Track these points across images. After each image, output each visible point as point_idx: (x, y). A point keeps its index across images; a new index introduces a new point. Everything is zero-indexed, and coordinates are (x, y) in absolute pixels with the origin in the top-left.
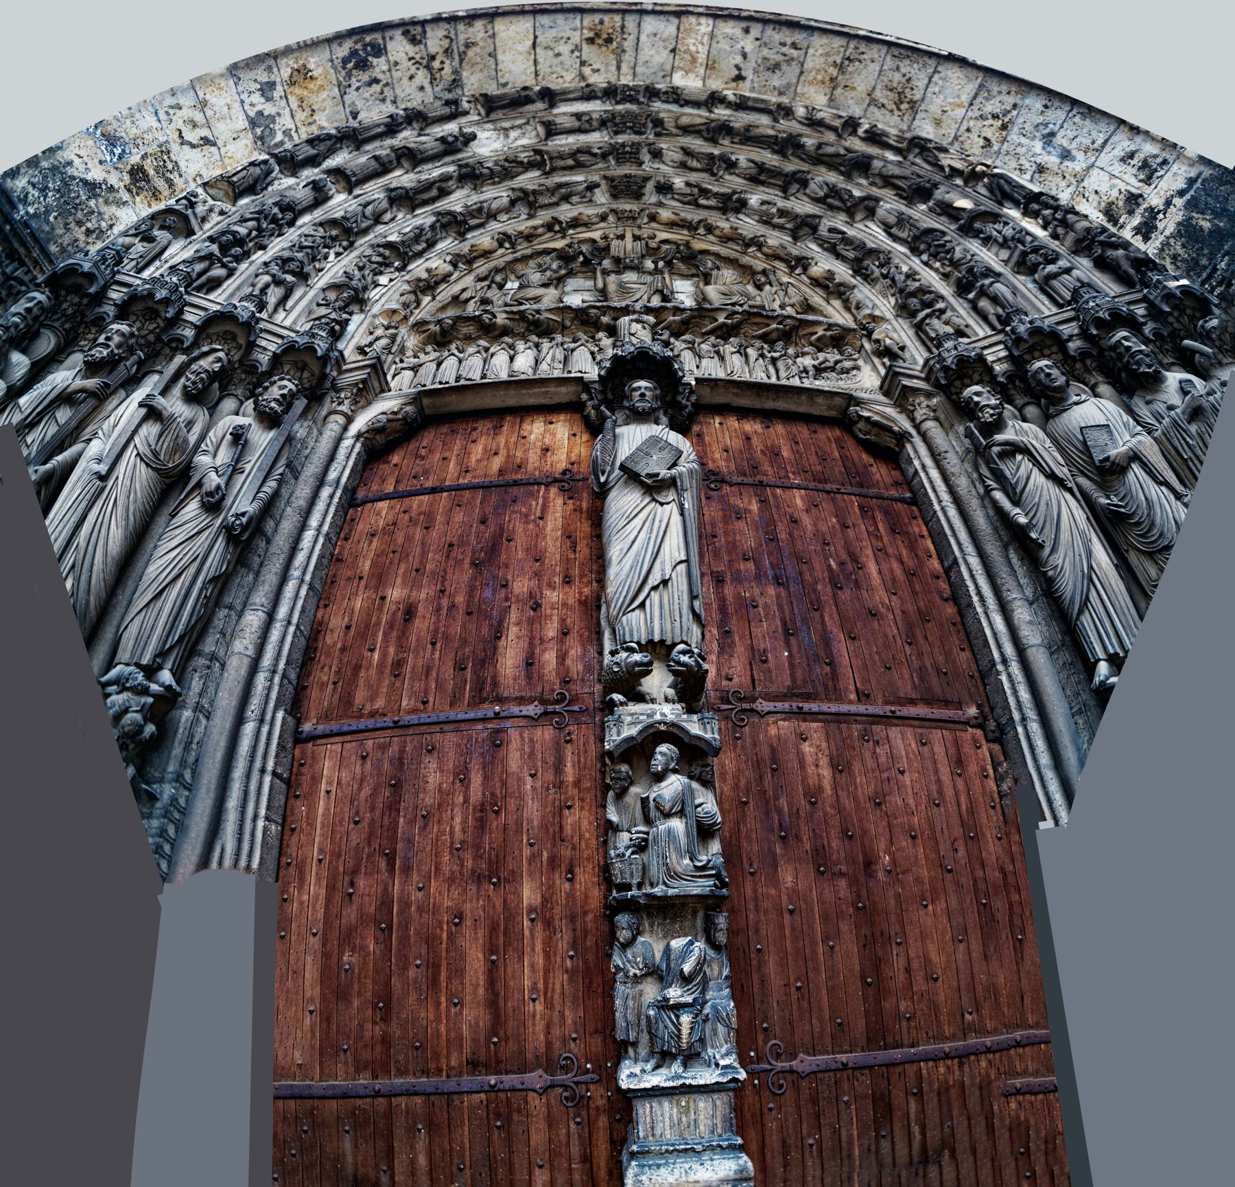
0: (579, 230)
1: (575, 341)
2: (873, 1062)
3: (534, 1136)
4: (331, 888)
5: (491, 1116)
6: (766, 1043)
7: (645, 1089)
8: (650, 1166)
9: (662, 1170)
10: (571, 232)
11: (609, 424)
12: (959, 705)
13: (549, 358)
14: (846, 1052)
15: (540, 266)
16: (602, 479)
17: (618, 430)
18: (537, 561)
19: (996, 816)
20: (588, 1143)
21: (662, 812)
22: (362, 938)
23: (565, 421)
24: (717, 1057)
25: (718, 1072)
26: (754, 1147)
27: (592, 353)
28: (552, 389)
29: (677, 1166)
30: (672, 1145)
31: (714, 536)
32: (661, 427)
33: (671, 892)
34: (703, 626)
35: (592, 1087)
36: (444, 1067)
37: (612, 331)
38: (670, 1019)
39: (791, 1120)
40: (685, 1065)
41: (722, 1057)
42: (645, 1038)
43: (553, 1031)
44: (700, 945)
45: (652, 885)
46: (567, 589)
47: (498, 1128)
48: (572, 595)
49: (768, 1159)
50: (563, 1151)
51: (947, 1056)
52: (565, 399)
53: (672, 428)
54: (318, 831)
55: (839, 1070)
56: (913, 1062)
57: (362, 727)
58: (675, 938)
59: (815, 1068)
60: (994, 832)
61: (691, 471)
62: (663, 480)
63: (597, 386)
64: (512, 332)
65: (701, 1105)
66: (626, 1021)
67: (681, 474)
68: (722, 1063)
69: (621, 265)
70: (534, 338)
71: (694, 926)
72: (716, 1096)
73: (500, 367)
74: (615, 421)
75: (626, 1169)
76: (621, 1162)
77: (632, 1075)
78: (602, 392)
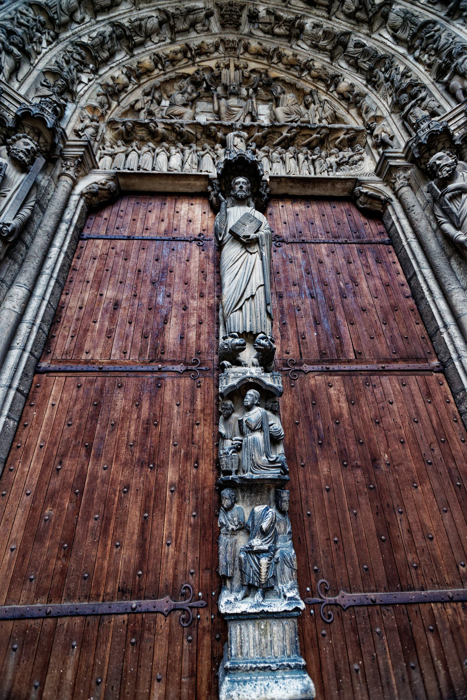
0: (203, 58)
1: (203, 150)
2: (394, 601)
3: (157, 652)
4: (46, 465)
5: (129, 634)
6: (317, 581)
7: (237, 614)
8: (238, 682)
9: (248, 686)
10: (198, 59)
11: (223, 206)
12: (426, 360)
13: (189, 161)
14: (373, 591)
15: (181, 88)
16: (220, 239)
17: (228, 210)
18: (186, 284)
19: (459, 427)
20: (195, 659)
21: (250, 428)
22: (61, 498)
23: (199, 204)
24: (285, 590)
25: (286, 602)
26: (314, 668)
27: (213, 159)
28: (192, 182)
29: (259, 683)
30: (255, 663)
31: (278, 273)
32: (251, 208)
33: (255, 476)
34: (272, 319)
35: (201, 611)
36: (102, 593)
37: (224, 144)
38: (254, 560)
39: (339, 645)
40: (264, 596)
41: (288, 590)
42: (237, 574)
43: (178, 567)
44: (272, 510)
45: (244, 472)
46: (201, 300)
47: (133, 644)
48: (204, 303)
49: (326, 682)
50: (177, 666)
51: (451, 600)
52: (199, 190)
53: (256, 209)
54: (43, 428)
55: (370, 605)
56: (425, 603)
57: (79, 369)
58: (257, 505)
59: (352, 603)
60: (459, 437)
61: (267, 235)
62: (252, 239)
63: (216, 181)
64: (168, 139)
65: (275, 628)
66: (226, 561)
67: (261, 236)
68: (289, 595)
69: (230, 92)
70: (180, 145)
71: (269, 498)
72: (285, 622)
73: (162, 165)
74: (227, 204)
75: (221, 685)
76: (217, 677)
77: (228, 602)
78: (219, 185)
